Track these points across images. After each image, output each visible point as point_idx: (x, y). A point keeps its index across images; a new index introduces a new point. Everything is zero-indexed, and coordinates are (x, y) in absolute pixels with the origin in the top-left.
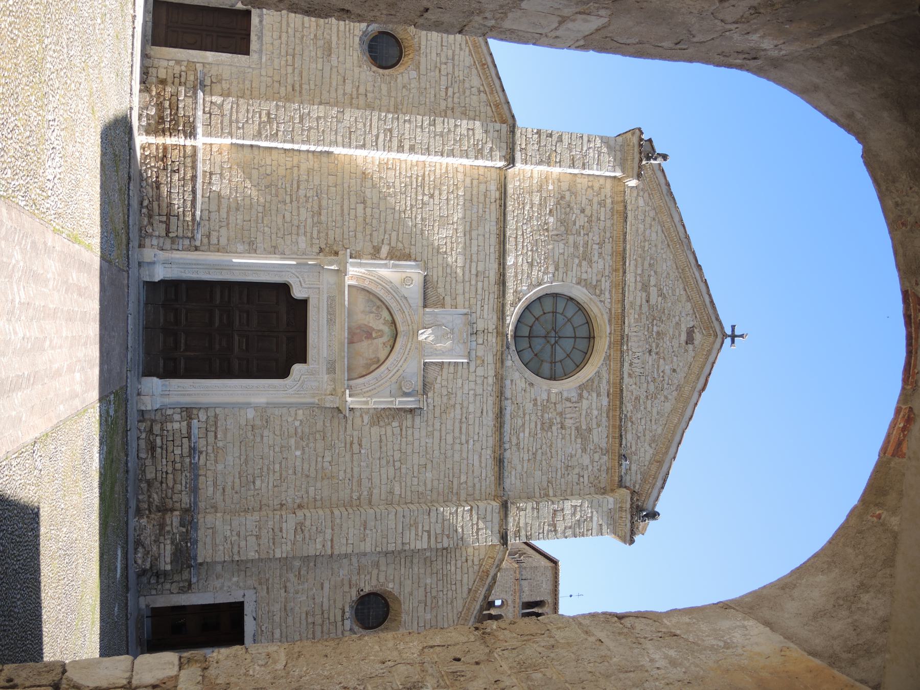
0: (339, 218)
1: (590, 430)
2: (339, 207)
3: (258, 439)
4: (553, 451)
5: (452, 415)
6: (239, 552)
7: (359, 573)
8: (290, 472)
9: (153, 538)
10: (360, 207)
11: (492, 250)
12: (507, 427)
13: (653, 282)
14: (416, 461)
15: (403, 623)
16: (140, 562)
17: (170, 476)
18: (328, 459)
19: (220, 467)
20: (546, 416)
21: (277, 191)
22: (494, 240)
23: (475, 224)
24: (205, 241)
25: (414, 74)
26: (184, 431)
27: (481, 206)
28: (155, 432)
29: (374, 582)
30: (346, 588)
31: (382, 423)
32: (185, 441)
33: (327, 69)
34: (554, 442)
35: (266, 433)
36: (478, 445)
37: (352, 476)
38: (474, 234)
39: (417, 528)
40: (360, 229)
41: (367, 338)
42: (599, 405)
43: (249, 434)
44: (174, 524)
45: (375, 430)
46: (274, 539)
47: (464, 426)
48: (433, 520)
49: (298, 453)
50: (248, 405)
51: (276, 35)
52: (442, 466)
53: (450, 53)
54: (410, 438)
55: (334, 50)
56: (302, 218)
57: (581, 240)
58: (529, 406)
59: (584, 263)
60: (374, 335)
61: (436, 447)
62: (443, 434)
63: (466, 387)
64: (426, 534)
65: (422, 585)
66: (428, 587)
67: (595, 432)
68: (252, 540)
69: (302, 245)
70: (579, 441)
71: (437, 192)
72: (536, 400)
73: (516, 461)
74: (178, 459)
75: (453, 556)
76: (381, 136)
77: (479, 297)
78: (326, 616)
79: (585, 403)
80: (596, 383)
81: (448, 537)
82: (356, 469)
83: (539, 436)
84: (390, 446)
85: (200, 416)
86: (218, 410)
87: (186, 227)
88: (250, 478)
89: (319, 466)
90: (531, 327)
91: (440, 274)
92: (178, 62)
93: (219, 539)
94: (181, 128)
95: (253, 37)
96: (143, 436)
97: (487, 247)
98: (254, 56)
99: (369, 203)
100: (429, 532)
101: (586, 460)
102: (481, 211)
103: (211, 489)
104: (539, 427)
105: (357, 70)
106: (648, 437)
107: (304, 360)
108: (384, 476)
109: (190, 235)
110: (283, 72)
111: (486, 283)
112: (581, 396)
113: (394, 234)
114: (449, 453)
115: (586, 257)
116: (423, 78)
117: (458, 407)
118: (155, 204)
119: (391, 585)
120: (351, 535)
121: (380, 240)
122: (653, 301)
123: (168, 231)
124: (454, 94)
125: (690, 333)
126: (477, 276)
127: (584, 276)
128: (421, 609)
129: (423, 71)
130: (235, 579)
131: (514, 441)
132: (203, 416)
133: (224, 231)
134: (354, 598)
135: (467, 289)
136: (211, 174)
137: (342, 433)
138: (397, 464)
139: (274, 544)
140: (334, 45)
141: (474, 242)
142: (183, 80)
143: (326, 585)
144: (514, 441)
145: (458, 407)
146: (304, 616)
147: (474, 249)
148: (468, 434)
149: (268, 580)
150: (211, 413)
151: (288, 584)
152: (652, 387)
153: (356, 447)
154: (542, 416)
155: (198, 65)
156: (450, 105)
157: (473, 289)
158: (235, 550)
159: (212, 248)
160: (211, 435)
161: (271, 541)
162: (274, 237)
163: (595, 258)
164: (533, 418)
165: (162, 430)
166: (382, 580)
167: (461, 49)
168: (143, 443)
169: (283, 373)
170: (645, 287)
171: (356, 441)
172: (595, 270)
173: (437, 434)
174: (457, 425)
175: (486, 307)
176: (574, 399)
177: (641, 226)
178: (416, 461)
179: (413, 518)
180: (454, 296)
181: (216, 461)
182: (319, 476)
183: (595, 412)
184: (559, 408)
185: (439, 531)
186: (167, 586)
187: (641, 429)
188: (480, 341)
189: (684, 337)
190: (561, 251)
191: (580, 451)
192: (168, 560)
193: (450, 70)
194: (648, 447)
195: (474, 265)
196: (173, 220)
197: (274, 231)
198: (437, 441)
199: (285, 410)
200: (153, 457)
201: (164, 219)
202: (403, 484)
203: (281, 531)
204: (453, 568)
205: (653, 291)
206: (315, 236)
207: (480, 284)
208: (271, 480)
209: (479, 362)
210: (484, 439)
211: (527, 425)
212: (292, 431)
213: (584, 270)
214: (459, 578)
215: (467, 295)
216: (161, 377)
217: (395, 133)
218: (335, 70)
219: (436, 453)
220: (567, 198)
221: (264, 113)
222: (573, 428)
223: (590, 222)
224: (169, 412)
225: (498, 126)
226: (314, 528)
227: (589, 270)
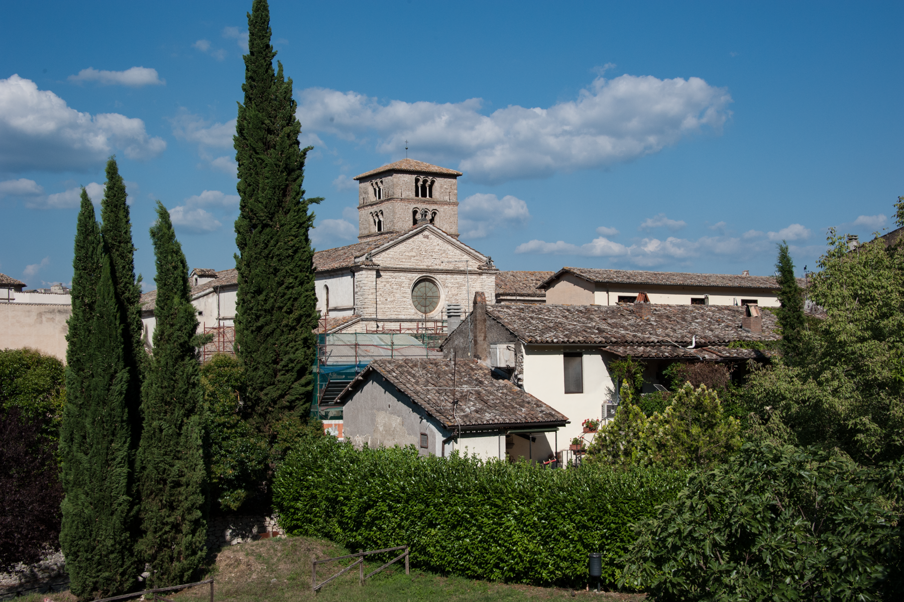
79: (450, 285)
122: (414, 254)
205: (411, 254)
223: (388, 282)
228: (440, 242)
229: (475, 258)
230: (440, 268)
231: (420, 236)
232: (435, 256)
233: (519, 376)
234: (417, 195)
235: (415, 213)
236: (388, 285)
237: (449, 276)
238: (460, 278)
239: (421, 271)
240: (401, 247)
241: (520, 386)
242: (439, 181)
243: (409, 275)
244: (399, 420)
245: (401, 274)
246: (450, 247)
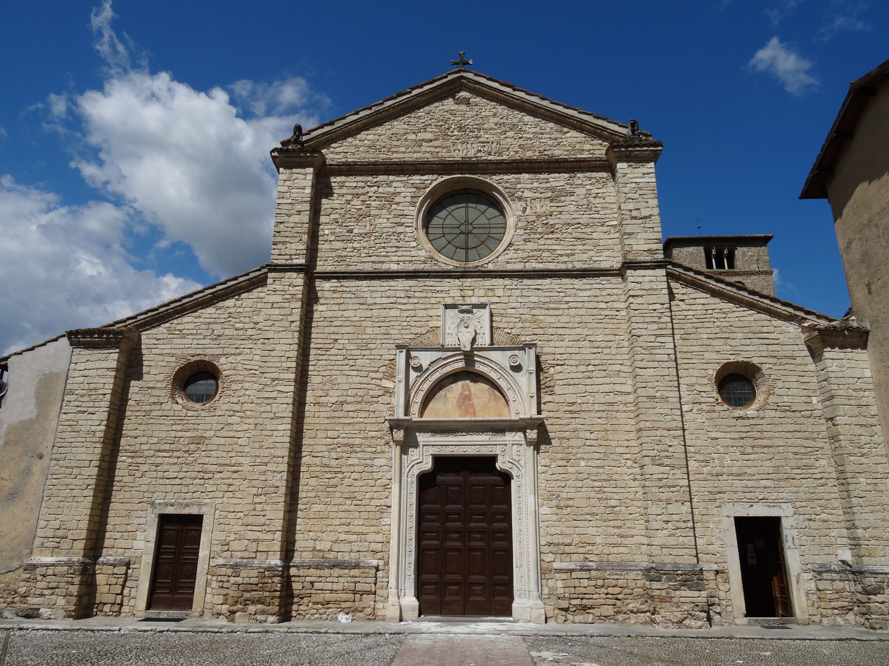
0: (357, 427)
1: (552, 189)
2: (347, 428)
3: (570, 503)
4: (574, 221)
5: (542, 318)
6: (684, 522)
7: (700, 403)
8: (601, 471)
9: (674, 609)
10: (346, 407)
11: (385, 284)
12: (552, 266)
13: (413, 137)
14: (588, 351)
15: (748, 360)
16: (700, 623)
17: (610, 590)
18: (588, 435)
19: (598, 540)
20: (540, 230)
21: (332, 487)
22: (376, 283)
23: (361, 301)
24: (379, 555)
25: (223, 360)
26: (565, 576)
27: (344, 295)
28: (567, 606)
29: (708, 388)
30: (715, 415)
31: (552, 383)
32: (574, 575)
33: (216, 440)
34: (564, 221)
35: (564, 495)
36: (569, 292)
37: (604, 411)
38: (370, 301)
39: (653, 348)
40: (366, 407)
41: (470, 399)
42: (528, 181)
43: (565, 511)
44: (659, 587)
45: (557, 389)
46: (670, 487)
47: (552, 306)
48: (644, 332)
49: (583, 463)
50: (536, 513)
51: (185, 489)
52: (590, 325)
53: (203, 327)
54: (565, 356)
55: (199, 434)
56: (356, 461)
58: (530, 246)
59: (397, 200)
60: (467, 393)
61: (573, 332)
62: (560, 325)
63: (514, 305)
64: (659, 339)
65: (708, 343)
66: (710, 336)
67: (554, 184)
68: (671, 509)
69: (382, 462)
70: (563, 198)
71: (333, 336)
72: (525, 241)
73: (585, 257)
74: (593, 583)
75: (679, 313)
76: (278, 388)
77: (429, 295)
78: (745, 435)
79: (527, 194)
80: (507, 185)
81: (660, 318)
82: (596, 407)
83: (559, 236)
84: (574, 375)
85: (549, 560)
86: (543, 543)
87: (366, 575)
88: (608, 510)
89: (593, 442)
90: (457, 248)
91: (408, 332)
92: (208, 584)
93: (672, 541)
94: (270, 581)
95: (186, 511)
96: (570, 617)
97: (383, 289)
98: (204, 510)
99: (342, 399)
100: (657, 336)
101: (581, 191)
102: (349, 296)
103: (621, 549)
104: (550, 236)
105: (218, 412)
106: (558, 135)
107: (493, 459)
108: (602, 380)
109: (373, 571)
110: (219, 482)
111: (416, 289)
112: (520, 199)
113: (372, 375)
114: (578, 319)
115: (390, 199)
116: (227, 351)
117: (533, 312)
118: (344, 605)
119: (711, 372)
120: (662, 411)
121: (377, 388)
122: (429, 136)
123: (369, 593)
124: (241, 322)
125: (459, 102)
126: (409, 297)
127: (408, 199)
128: (733, 342)
129: (220, 351)
130: (711, 525)
131: (565, 259)
132: (549, 558)
133: (370, 538)
134: (726, 407)
135: (422, 306)
136: (314, 549)
137: (561, 422)
138: (591, 368)
139: (674, 487)
140: (195, 434)
141: (378, 301)
142: (225, 579)
143: (713, 435)
144: (565, 259)
145: (533, 312)
146: (745, 457)
147: (384, 300)
148: (560, 302)
149: (711, 493)
150: (546, 549)
151: (714, 472)
153: (574, 408)
154: (540, 233)
155: (211, 564)
156: (252, 325)
157: (421, 301)
158: (683, 525)
159: (386, 549)
160: (568, 549)
161: (672, 489)
162: (375, 489)
163: (392, 190)
164: (542, 242)
165: (563, 598)
166: (705, 381)
167: (199, 317)
168: (579, 618)
169: (506, 478)
170: (419, 143)
171: (570, 409)
172: (403, 189)
173: (560, 331)
174: (551, 312)
175: (438, 289)
176: (524, 205)
177: (361, 149)
178: (588, 351)
179: (643, 351)
180: (428, 318)
181: (593, 544)
182: (605, 443)
185: (655, 326)
186: (722, 594)
187: (550, 142)
188: (470, 293)
189: (463, 107)
190: (385, 220)
191: (572, 198)
192: (696, 594)
193: (220, 326)
194: (568, 135)
195: (399, 300)
196: (359, 587)
197: (369, 489)
198: (567, 331)
199: (542, 477)
200: (591, 608)
201: (358, 596)
202: (610, 362)
203: (661, 479)
204: (691, 313)
205: (421, 136)
206: (374, 449)
207: (417, 294)
208: (610, 490)
209: (490, 294)
210: (564, 287)
211: (550, 247)
212: (561, 470)
213: (403, 200)
214: (700, 307)
215: (428, 306)
216: (512, 599)
217: (275, 376)
218: (219, 433)
219: (579, 331)
220: (337, 216)
221: (257, 500)
222: (552, 204)
223: (358, 195)
224: (546, 591)
225: (269, 281)
226: (656, 447)
227: (402, 194)
228: (502, 110)
231: (449, 104)
232: (484, 137)
234: (709, 265)
236: (356, 202)
238: (558, 180)
240: (398, 125)
243: (416, 179)
246: (528, 118)
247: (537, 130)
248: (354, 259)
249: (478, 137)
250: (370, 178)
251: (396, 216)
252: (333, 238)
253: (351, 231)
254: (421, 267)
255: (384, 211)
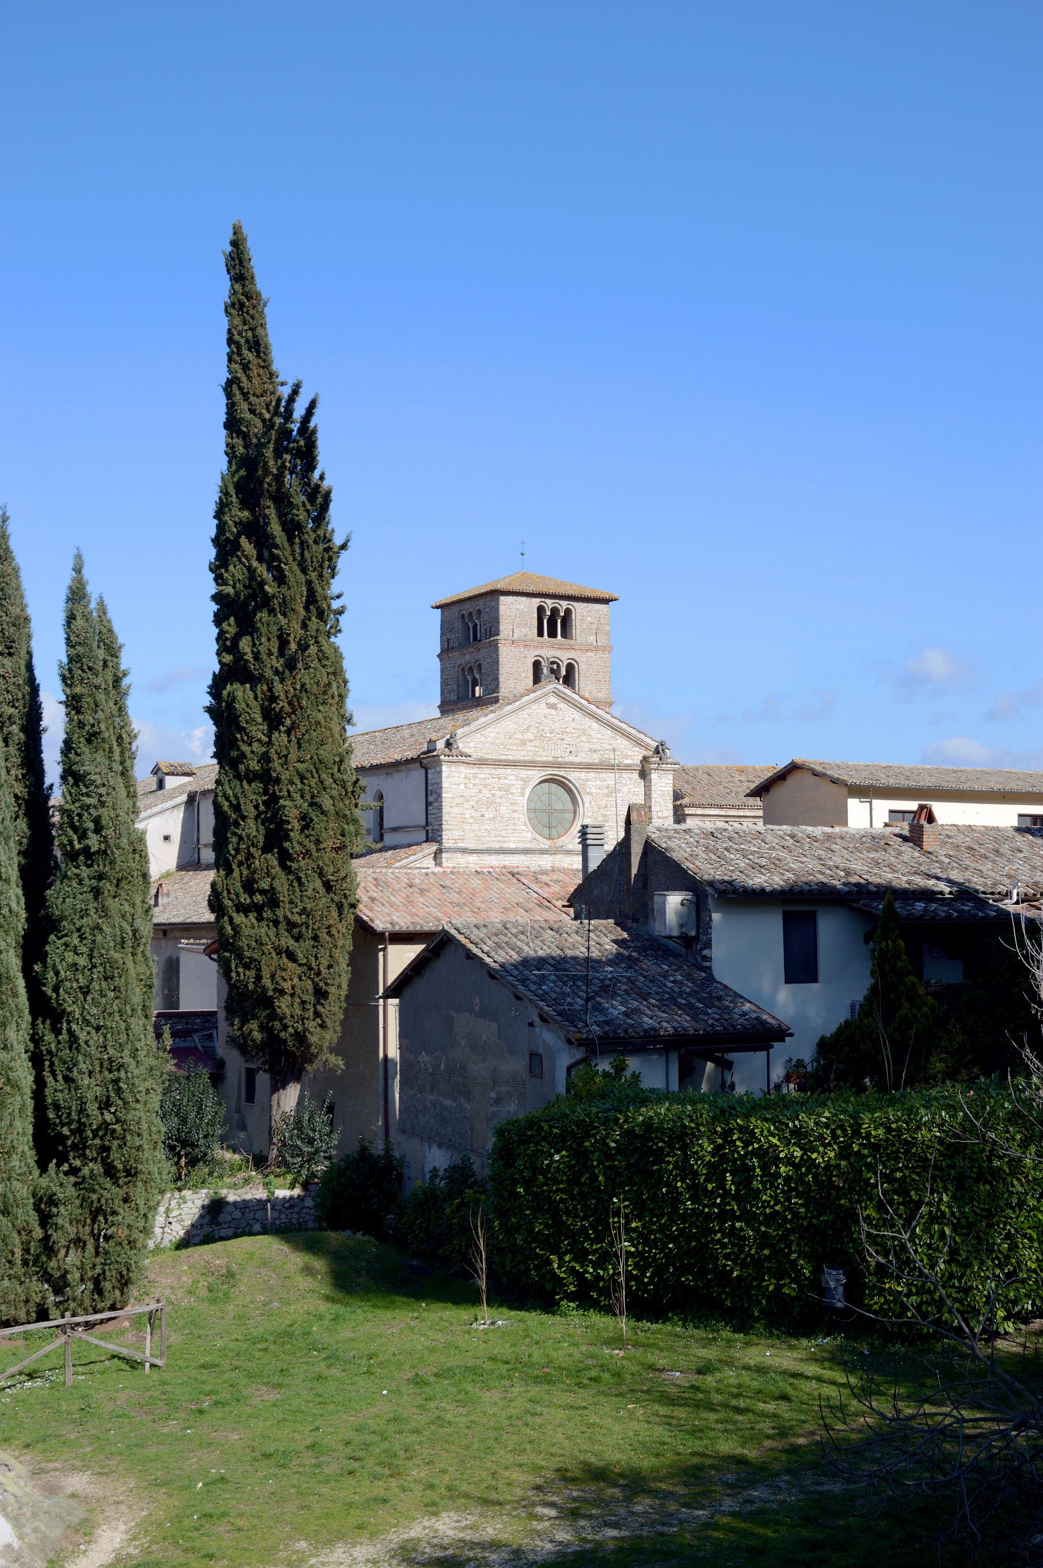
13: (520, 736)
57: (498, 793)
79: (594, 790)
122: (532, 737)
127: (519, 790)
152: (584, 738)
170: (524, 743)
183: (598, 782)
184: (596, 809)
189: (553, 712)
228: (577, 715)
229: (638, 743)
230: (577, 760)
232: (568, 740)
233: (706, 952)
234: (540, 634)
235: (537, 665)
237: (592, 775)
239: (545, 765)
241: (708, 970)
242: (580, 610)
243: (524, 773)
244: (494, 1026)
245: (509, 771)
246: (595, 725)
247: (599, 736)
248: (487, 839)
249: (562, 740)
250: (493, 771)
251: (512, 804)
252: (472, 821)
253: (483, 816)
254: (529, 846)
255: (504, 800)
